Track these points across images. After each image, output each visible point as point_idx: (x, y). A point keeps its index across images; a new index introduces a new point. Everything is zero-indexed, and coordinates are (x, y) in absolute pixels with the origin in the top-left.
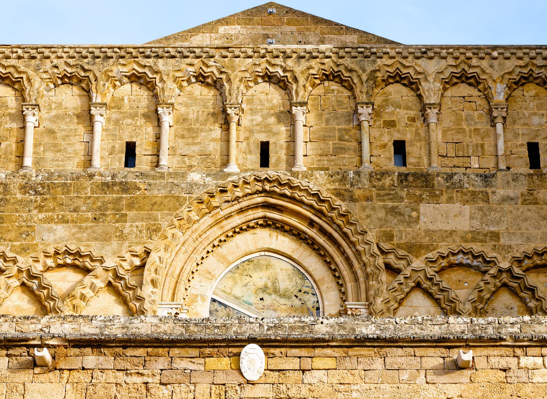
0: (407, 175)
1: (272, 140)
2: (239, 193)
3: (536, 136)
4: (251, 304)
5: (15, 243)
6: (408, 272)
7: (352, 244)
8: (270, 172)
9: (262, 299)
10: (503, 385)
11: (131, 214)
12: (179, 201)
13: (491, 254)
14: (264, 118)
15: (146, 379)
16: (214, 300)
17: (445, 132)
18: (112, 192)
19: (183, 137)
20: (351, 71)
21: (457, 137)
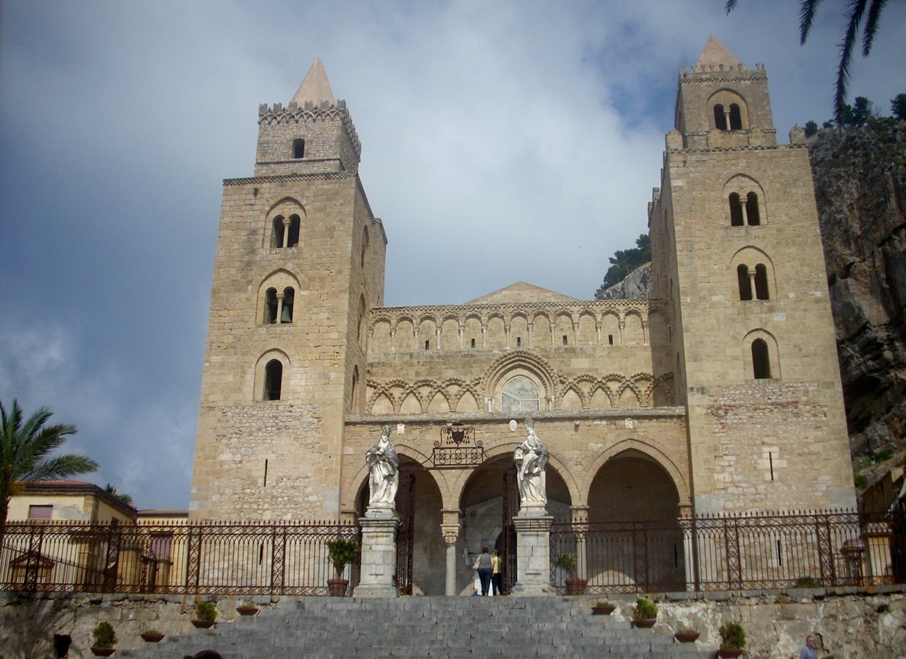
6: (567, 383)
8: (521, 349)
13: (595, 376)
17: (580, 332)
21: (585, 334)
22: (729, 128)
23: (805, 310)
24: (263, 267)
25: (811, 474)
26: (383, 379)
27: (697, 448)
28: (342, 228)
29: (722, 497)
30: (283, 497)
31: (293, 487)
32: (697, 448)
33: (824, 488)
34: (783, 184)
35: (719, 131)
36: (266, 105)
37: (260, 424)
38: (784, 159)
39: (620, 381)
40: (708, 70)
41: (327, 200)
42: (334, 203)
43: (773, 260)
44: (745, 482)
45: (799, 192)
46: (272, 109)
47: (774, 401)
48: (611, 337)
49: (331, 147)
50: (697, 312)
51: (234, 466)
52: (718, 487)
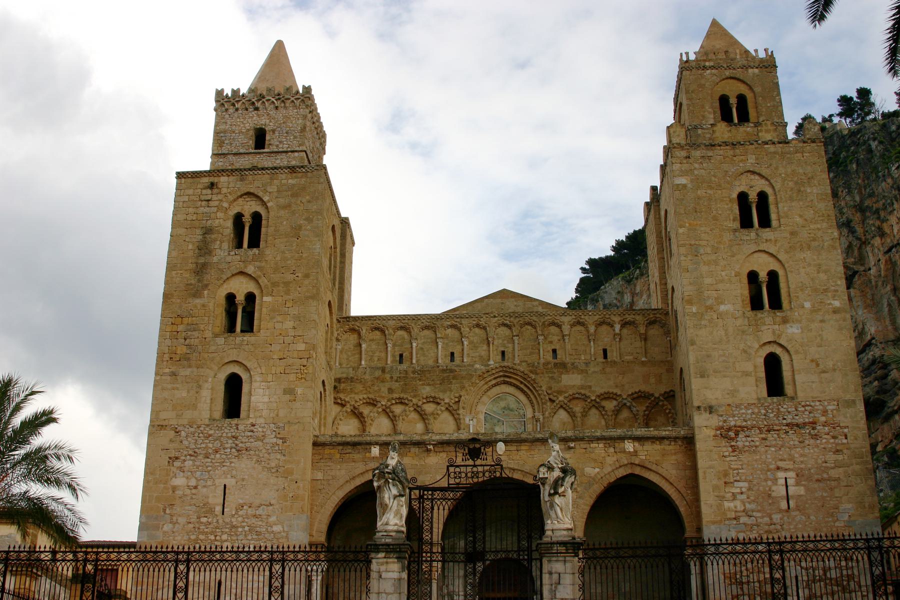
0: (557, 363)
1: (506, 350)
2: (494, 372)
3: (606, 346)
6: (557, 402)
7: (537, 391)
8: (506, 364)
11: (454, 381)
12: (472, 376)
13: (588, 394)
14: (503, 340)
16: (486, 413)
18: (447, 373)
19: (472, 349)
20: (535, 321)
22: (736, 120)
23: (822, 321)
24: (222, 271)
25: (831, 502)
26: (353, 396)
27: (705, 473)
28: (309, 227)
29: (734, 528)
30: (244, 527)
31: (255, 516)
32: (705, 473)
33: (846, 518)
34: (796, 183)
35: (726, 123)
36: (222, 90)
37: (217, 444)
38: (798, 155)
39: (615, 399)
40: (711, 56)
41: (292, 196)
42: (300, 199)
43: (786, 266)
44: (759, 511)
45: (815, 191)
46: (230, 95)
47: (789, 421)
48: (605, 351)
49: (295, 137)
50: (703, 322)
51: (188, 492)
52: (729, 516)
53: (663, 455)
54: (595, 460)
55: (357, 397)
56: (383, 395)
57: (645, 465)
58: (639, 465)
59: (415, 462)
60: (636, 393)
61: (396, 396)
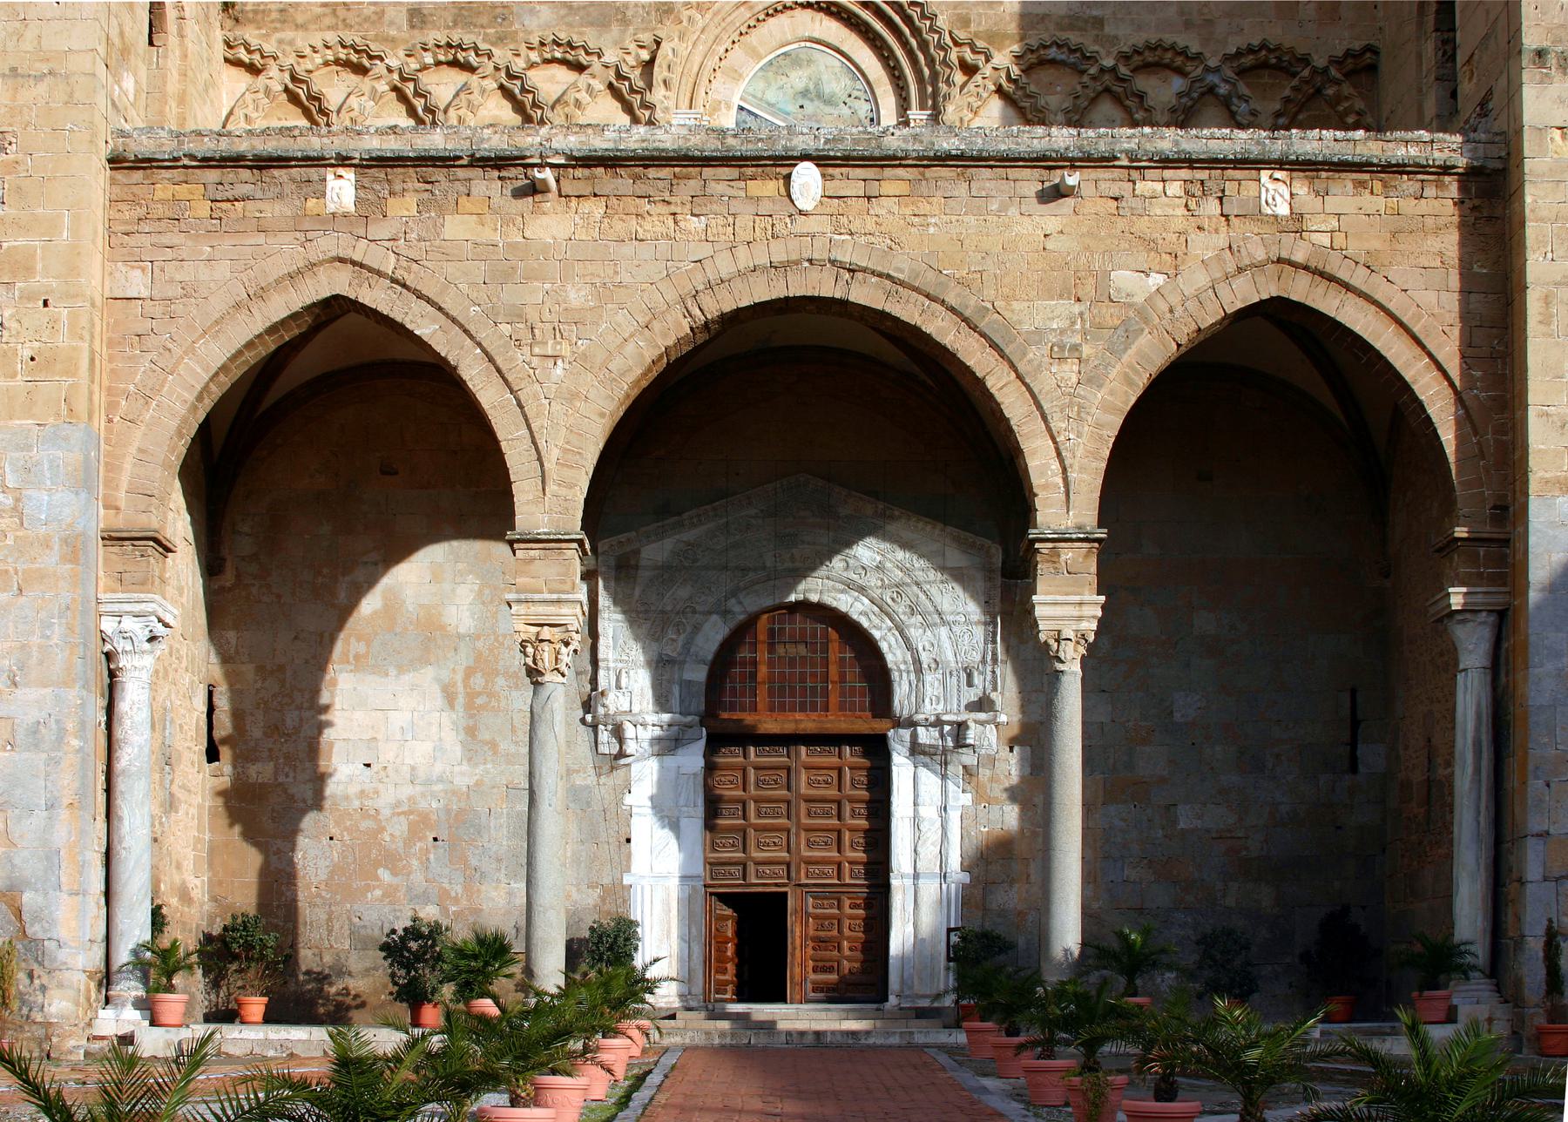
4: (788, 114)
5: (488, 31)
6: (987, 70)
9: (802, 107)
10: (1113, 219)
15: (673, 209)
16: (741, 108)
39: (1180, 72)
53: (1394, 234)
54: (1150, 244)
55: (302, 41)
56: (393, 32)
57: (1328, 269)
58: (1306, 268)
59: (488, 234)
60: (1251, 50)
61: (435, 35)
